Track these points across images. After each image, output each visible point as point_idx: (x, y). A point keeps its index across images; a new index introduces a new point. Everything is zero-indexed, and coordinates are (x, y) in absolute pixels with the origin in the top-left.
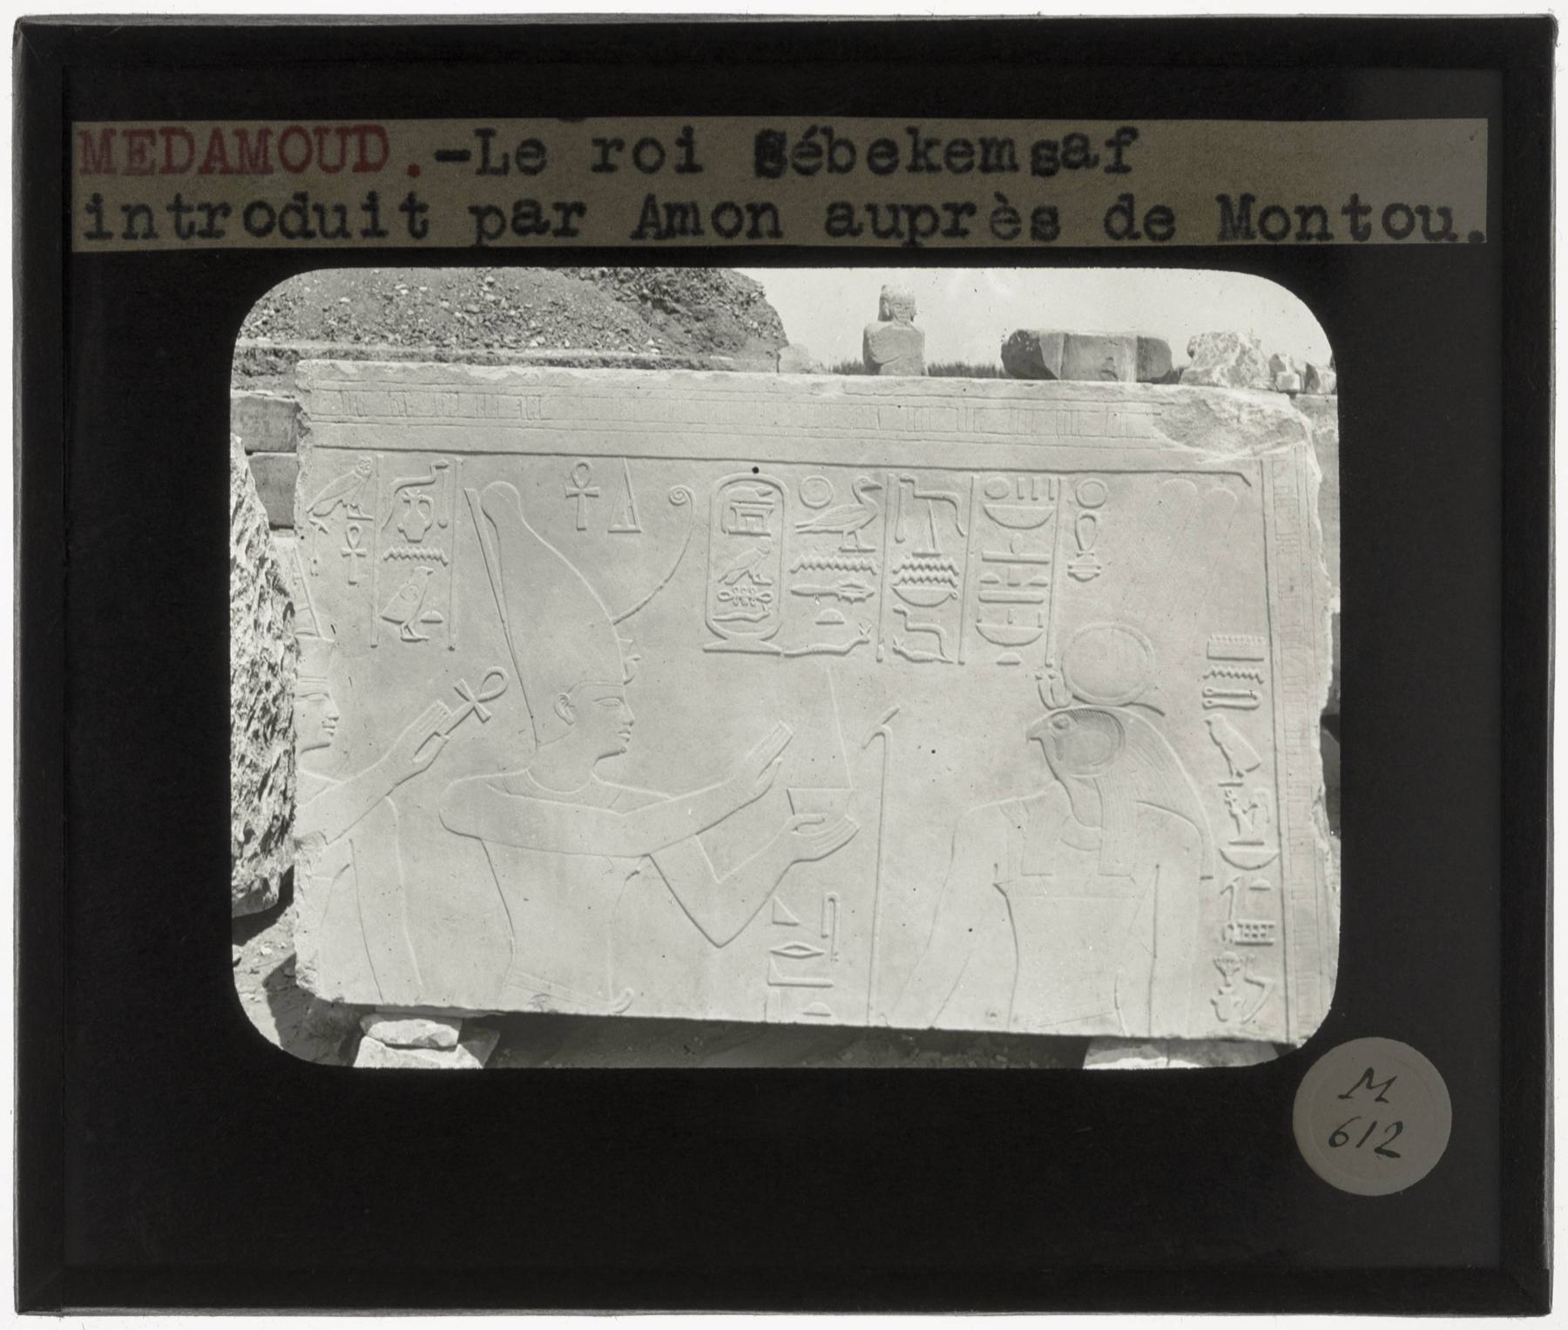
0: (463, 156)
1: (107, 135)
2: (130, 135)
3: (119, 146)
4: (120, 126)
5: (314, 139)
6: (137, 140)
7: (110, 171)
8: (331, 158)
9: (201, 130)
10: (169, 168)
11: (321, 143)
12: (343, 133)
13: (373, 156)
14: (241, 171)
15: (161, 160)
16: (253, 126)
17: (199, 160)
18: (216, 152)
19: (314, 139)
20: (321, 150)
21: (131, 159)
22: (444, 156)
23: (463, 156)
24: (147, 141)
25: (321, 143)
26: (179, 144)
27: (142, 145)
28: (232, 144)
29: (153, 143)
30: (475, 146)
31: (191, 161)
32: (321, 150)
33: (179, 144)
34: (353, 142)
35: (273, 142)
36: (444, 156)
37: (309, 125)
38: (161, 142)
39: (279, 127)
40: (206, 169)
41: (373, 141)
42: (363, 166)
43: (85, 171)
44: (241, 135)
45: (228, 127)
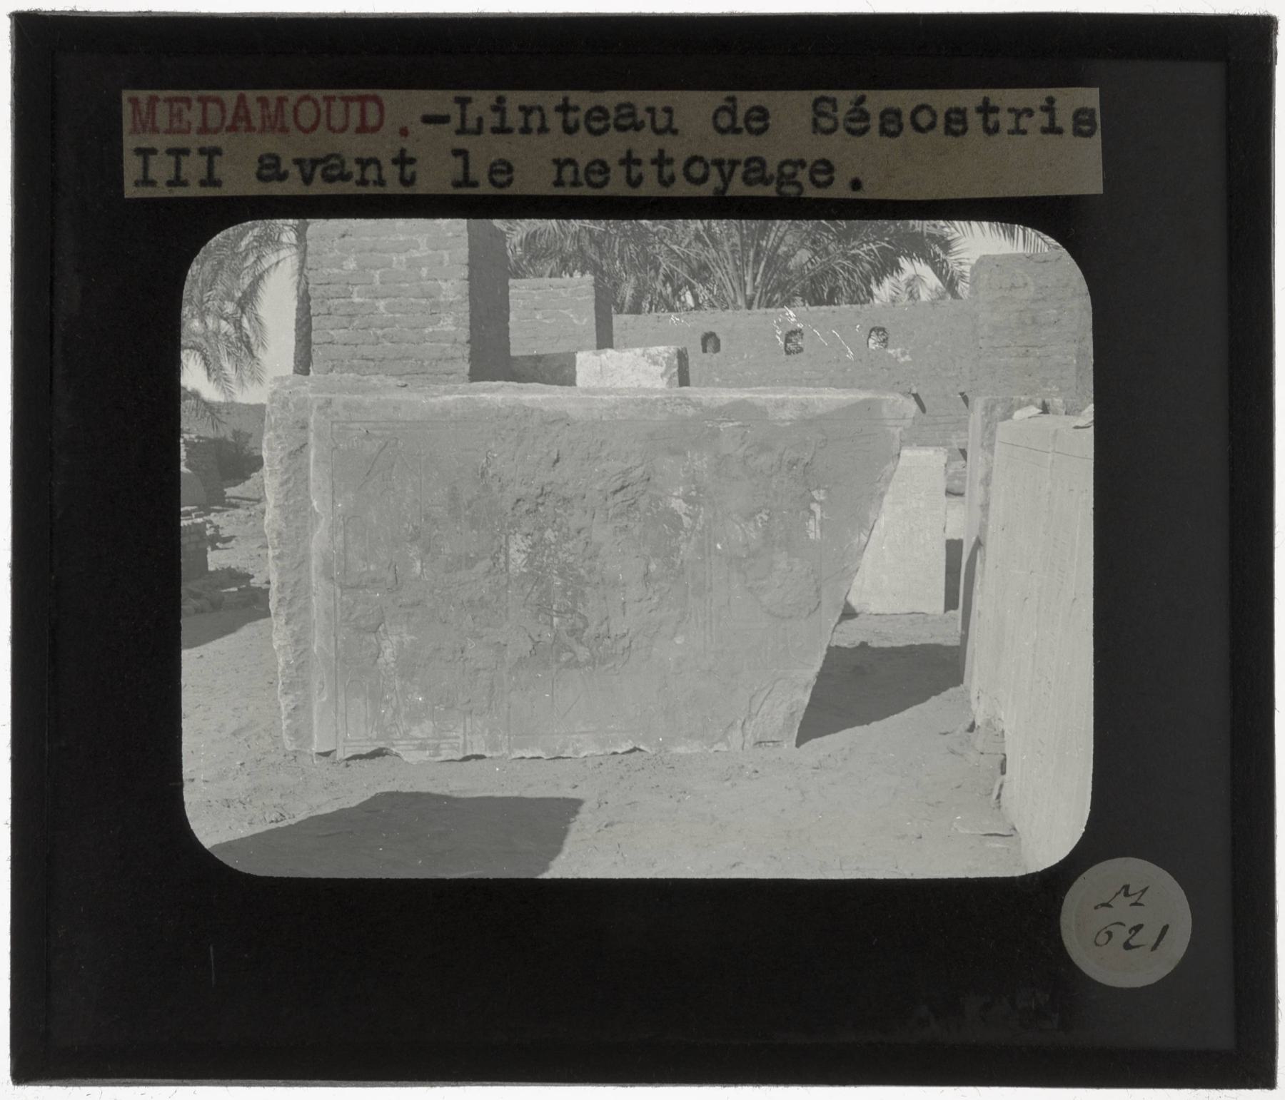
0: (444, 119)
1: (153, 100)
2: (170, 101)
4: (162, 94)
6: (176, 106)
11: (329, 107)
12: (347, 100)
13: (372, 120)
15: (196, 124)
16: (272, 95)
17: (228, 122)
18: (242, 113)
19: (323, 107)
20: (329, 116)
22: (427, 120)
23: (444, 119)
24: (184, 106)
25: (329, 107)
26: (213, 108)
27: (180, 111)
29: (189, 108)
30: (454, 111)
31: (222, 124)
32: (329, 116)
33: (213, 108)
35: (288, 108)
36: (427, 120)
37: (318, 94)
38: (196, 105)
39: (293, 95)
41: (372, 108)
44: (263, 102)
45: (251, 95)
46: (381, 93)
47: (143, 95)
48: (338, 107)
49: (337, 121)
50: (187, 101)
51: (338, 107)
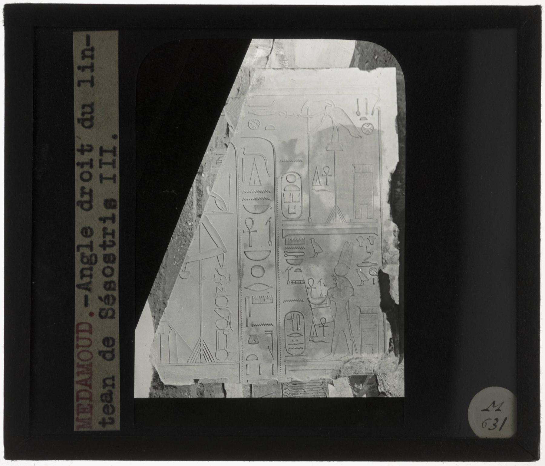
0: (86, 297)
4: (76, 416)
6: (80, 410)
7: (91, 419)
15: (88, 402)
16: (76, 370)
22: (86, 304)
26: (82, 394)
29: (81, 405)
34: (81, 335)
36: (86, 304)
38: (81, 401)
40: (90, 386)
41: (82, 327)
44: (78, 374)
45: (76, 378)
46: (76, 323)
47: (76, 424)
48: (81, 342)
49: (87, 342)
50: (78, 405)
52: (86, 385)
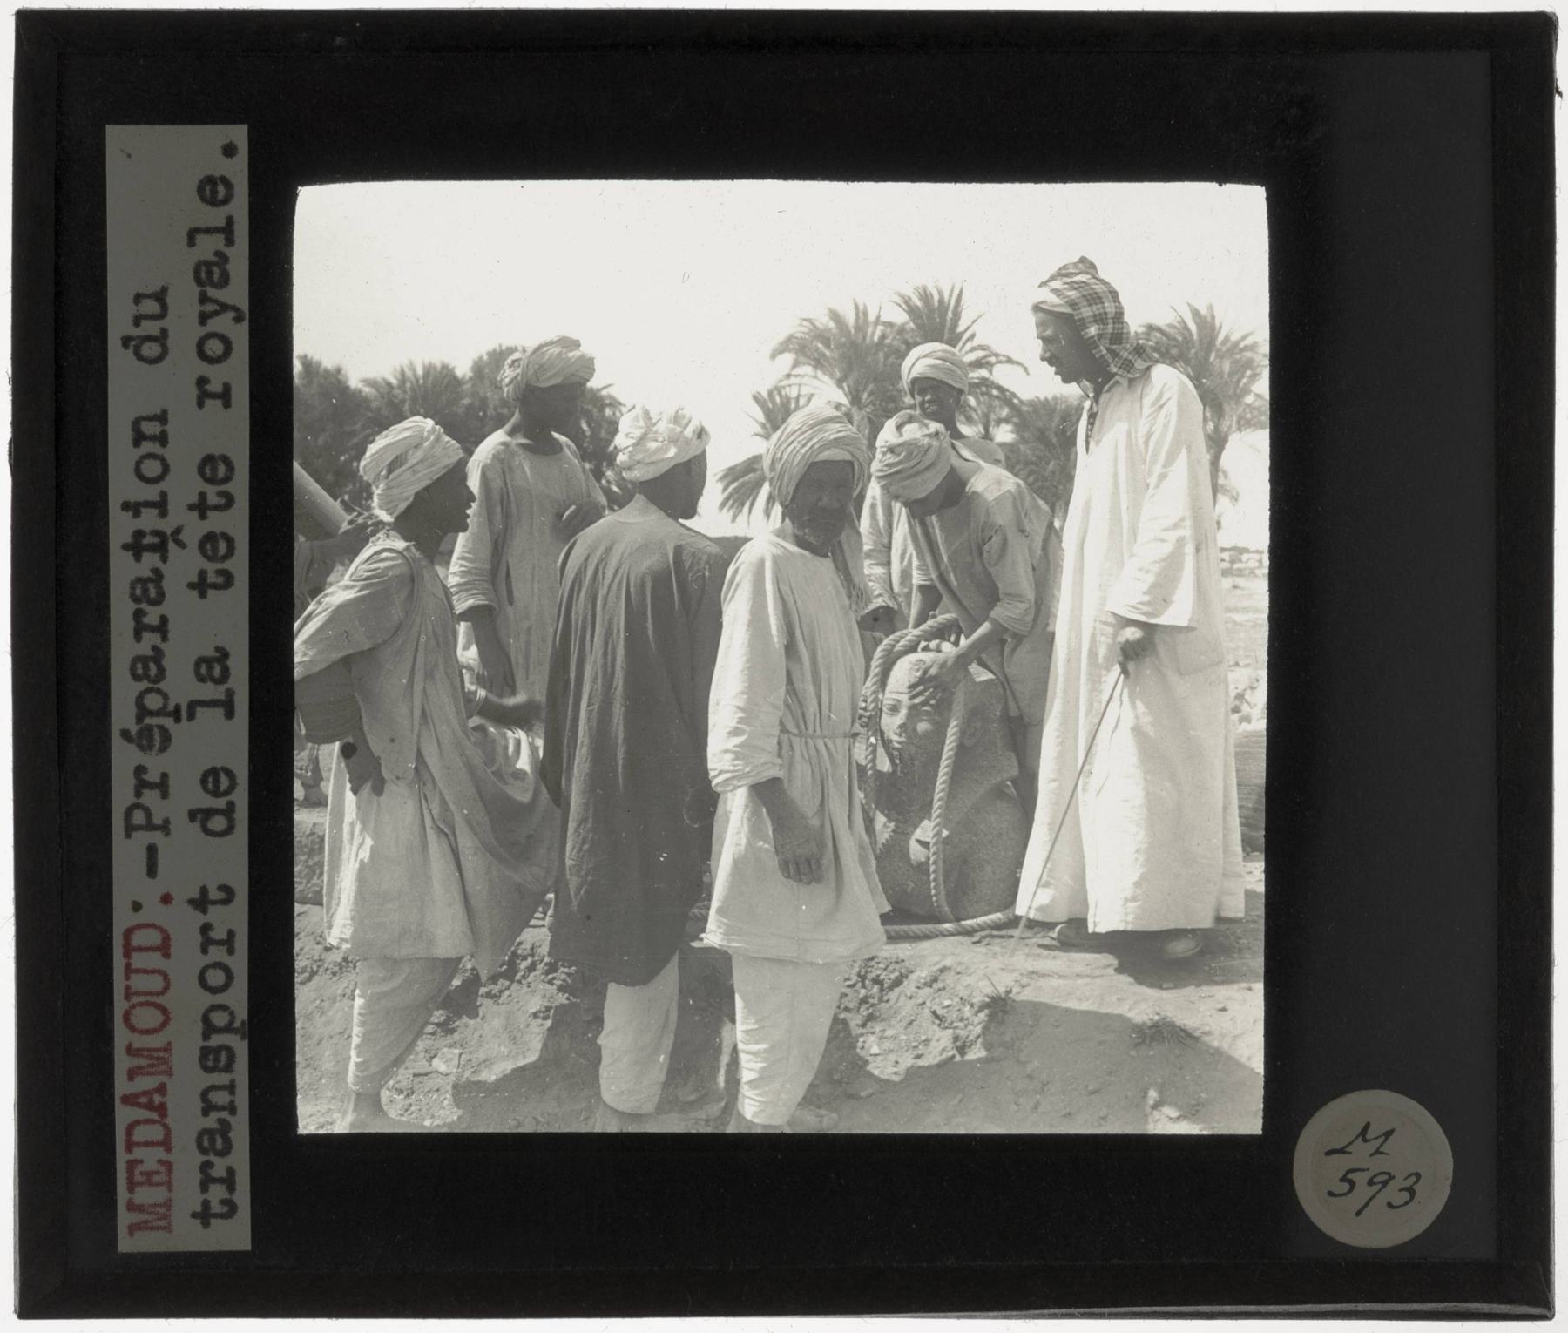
1: (131, 1207)
3: (144, 1195)
5: (136, 1000)
6: (138, 1178)
8: (156, 983)
9: (123, 1115)
10: (166, 1144)
11: (138, 993)
14: (169, 1073)
15: (160, 1153)
17: (154, 1116)
21: (159, 1184)
25: (138, 993)
26: (140, 1134)
28: (145, 1083)
33: (140, 1134)
34: (138, 960)
35: (141, 1041)
38: (138, 1153)
40: (162, 1110)
42: (165, 948)
43: (168, 1228)
44: (132, 1074)
45: (121, 1086)
47: (124, 1218)
51: (139, 982)
52: (149, 1106)
